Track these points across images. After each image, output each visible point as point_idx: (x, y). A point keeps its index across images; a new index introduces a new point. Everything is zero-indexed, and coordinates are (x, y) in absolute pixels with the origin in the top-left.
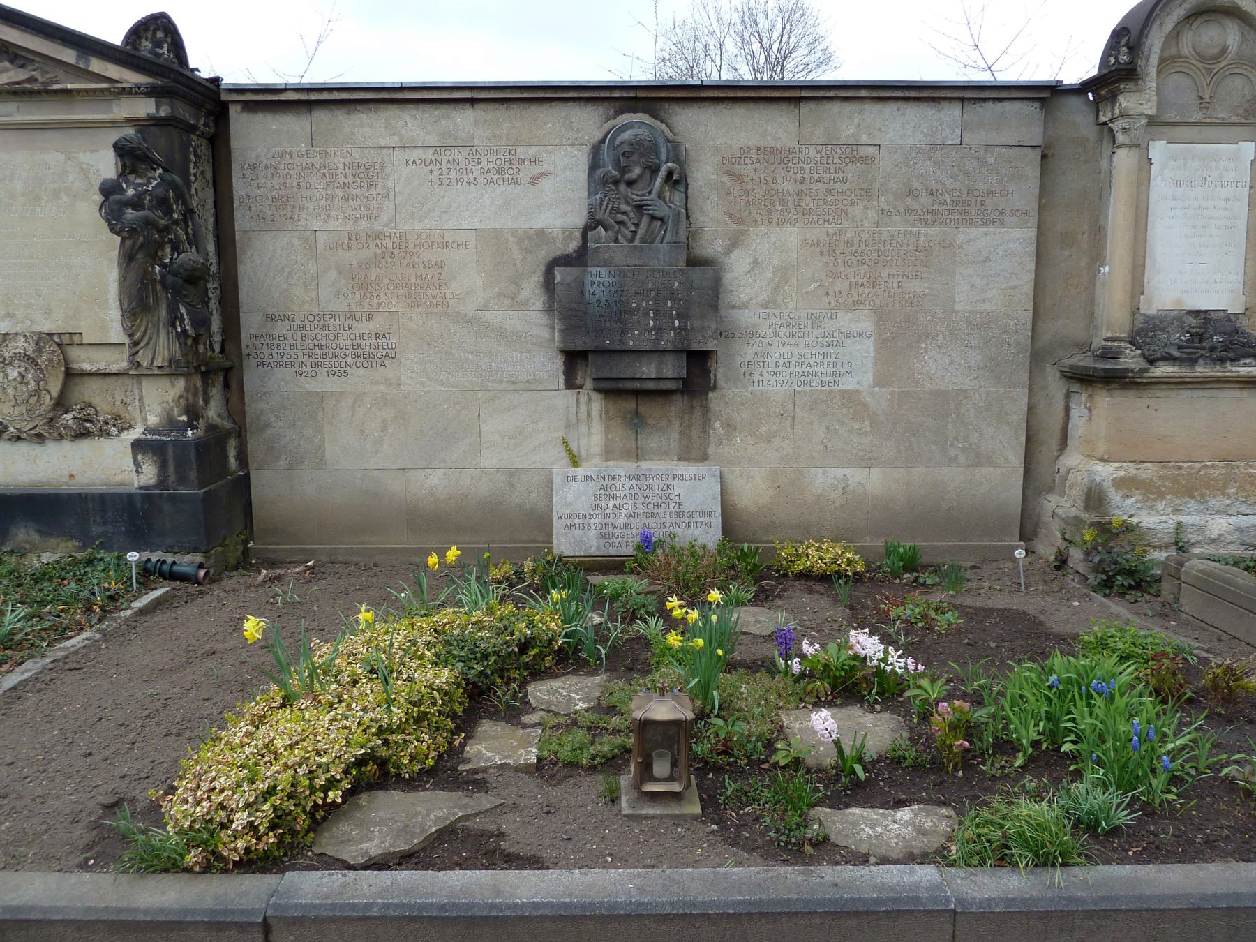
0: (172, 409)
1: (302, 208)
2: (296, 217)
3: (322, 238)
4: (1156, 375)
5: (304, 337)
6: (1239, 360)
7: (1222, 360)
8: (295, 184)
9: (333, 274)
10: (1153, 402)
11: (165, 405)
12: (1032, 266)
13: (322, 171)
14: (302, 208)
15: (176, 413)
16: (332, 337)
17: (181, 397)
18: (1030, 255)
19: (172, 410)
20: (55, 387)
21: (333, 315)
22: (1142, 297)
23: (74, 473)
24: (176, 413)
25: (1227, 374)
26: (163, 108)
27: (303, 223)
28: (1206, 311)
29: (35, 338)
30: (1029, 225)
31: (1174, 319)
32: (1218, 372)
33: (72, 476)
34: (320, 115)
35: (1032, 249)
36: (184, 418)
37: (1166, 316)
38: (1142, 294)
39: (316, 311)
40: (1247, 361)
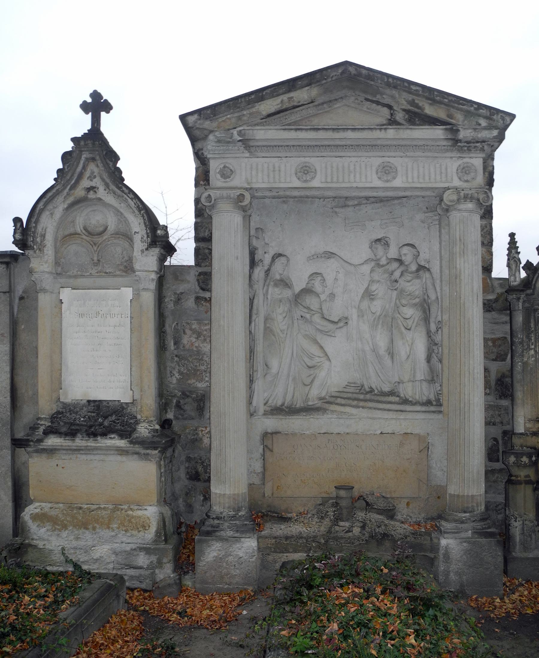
4: (49, 444)
6: (106, 435)
7: (95, 435)
10: (60, 462)
12: (8, 369)
18: (6, 362)
22: (61, 391)
25: (98, 445)
28: (95, 401)
30: (5, 342)
31: (83, 406)
32: (91, 443)
35: (7, 358)
37: (78, 404)
38: (61, 389)
40: (112, 436)
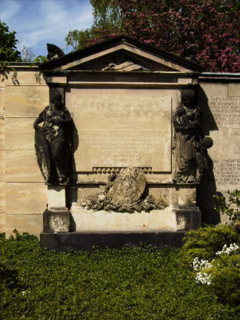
0: (191, 198)
1: (223, 119)
2: (221, 122)
3: (230, 131)
5: (222, 169)
8: (221, 110)
9: (234, 145)
11: (188, 197)
13: (232, 106)
14: (223, 119)
15: (192, 200)
16: (233, 169)
17: (194, 193)
19: (191, 198)
20: (142, 189)
21: (233, 161)
23: (145, 224)
24: (192, 200)
26: (195, 81)
27: (224, 125)
29: (135, 169)
33: (144, 226)
34: (231, 86)
36: (195, 202)
39: (227, 159)
